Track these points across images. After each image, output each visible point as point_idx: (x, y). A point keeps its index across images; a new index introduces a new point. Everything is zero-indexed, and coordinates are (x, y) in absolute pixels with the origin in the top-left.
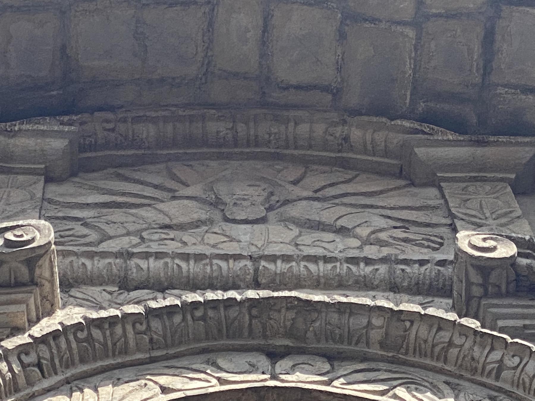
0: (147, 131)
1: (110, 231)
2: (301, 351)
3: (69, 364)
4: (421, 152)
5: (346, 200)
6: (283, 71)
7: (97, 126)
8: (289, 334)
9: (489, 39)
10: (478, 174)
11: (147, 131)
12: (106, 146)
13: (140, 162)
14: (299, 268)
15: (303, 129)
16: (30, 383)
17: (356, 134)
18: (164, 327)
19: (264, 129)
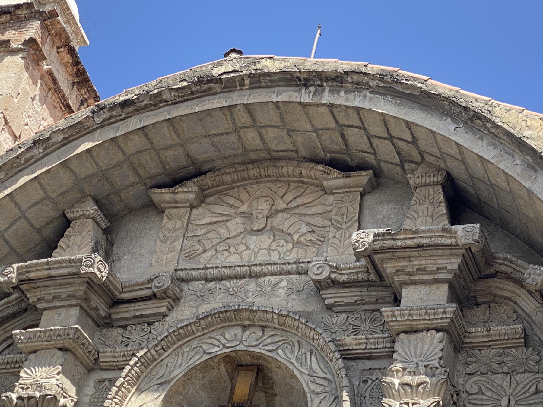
0: (227, 178)
1: (208, 245)
2: (254, 325)
3: (175, 343)
4: (325, 183)
5: (297, 211)
6: (273, 147)
7: (207, 180)
8: (249, 319)
9: (343, 136)
10: (348, 189)
11: (227, 178)
12: (213, 187)
13: (228, 189)
14: (265, 269)
15: (285, 170)
16: (160, 355)
17: (304, 172)
18: (206, 323)
19: (271, 171)
